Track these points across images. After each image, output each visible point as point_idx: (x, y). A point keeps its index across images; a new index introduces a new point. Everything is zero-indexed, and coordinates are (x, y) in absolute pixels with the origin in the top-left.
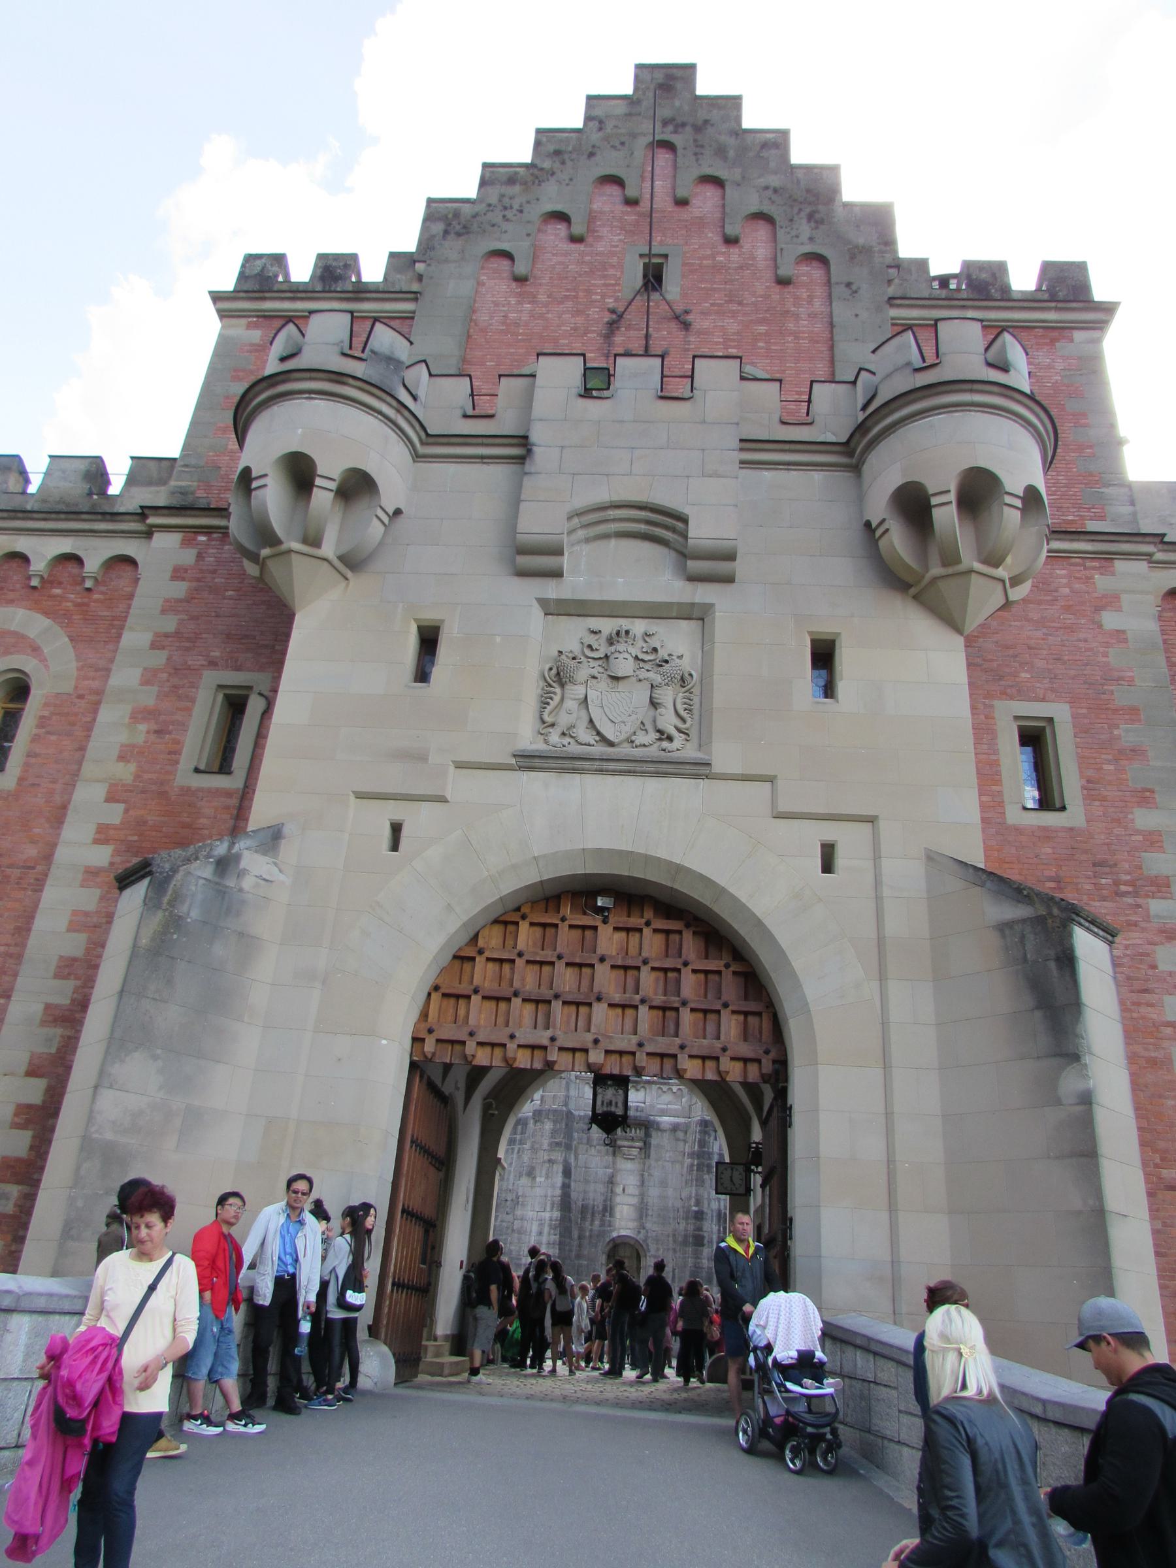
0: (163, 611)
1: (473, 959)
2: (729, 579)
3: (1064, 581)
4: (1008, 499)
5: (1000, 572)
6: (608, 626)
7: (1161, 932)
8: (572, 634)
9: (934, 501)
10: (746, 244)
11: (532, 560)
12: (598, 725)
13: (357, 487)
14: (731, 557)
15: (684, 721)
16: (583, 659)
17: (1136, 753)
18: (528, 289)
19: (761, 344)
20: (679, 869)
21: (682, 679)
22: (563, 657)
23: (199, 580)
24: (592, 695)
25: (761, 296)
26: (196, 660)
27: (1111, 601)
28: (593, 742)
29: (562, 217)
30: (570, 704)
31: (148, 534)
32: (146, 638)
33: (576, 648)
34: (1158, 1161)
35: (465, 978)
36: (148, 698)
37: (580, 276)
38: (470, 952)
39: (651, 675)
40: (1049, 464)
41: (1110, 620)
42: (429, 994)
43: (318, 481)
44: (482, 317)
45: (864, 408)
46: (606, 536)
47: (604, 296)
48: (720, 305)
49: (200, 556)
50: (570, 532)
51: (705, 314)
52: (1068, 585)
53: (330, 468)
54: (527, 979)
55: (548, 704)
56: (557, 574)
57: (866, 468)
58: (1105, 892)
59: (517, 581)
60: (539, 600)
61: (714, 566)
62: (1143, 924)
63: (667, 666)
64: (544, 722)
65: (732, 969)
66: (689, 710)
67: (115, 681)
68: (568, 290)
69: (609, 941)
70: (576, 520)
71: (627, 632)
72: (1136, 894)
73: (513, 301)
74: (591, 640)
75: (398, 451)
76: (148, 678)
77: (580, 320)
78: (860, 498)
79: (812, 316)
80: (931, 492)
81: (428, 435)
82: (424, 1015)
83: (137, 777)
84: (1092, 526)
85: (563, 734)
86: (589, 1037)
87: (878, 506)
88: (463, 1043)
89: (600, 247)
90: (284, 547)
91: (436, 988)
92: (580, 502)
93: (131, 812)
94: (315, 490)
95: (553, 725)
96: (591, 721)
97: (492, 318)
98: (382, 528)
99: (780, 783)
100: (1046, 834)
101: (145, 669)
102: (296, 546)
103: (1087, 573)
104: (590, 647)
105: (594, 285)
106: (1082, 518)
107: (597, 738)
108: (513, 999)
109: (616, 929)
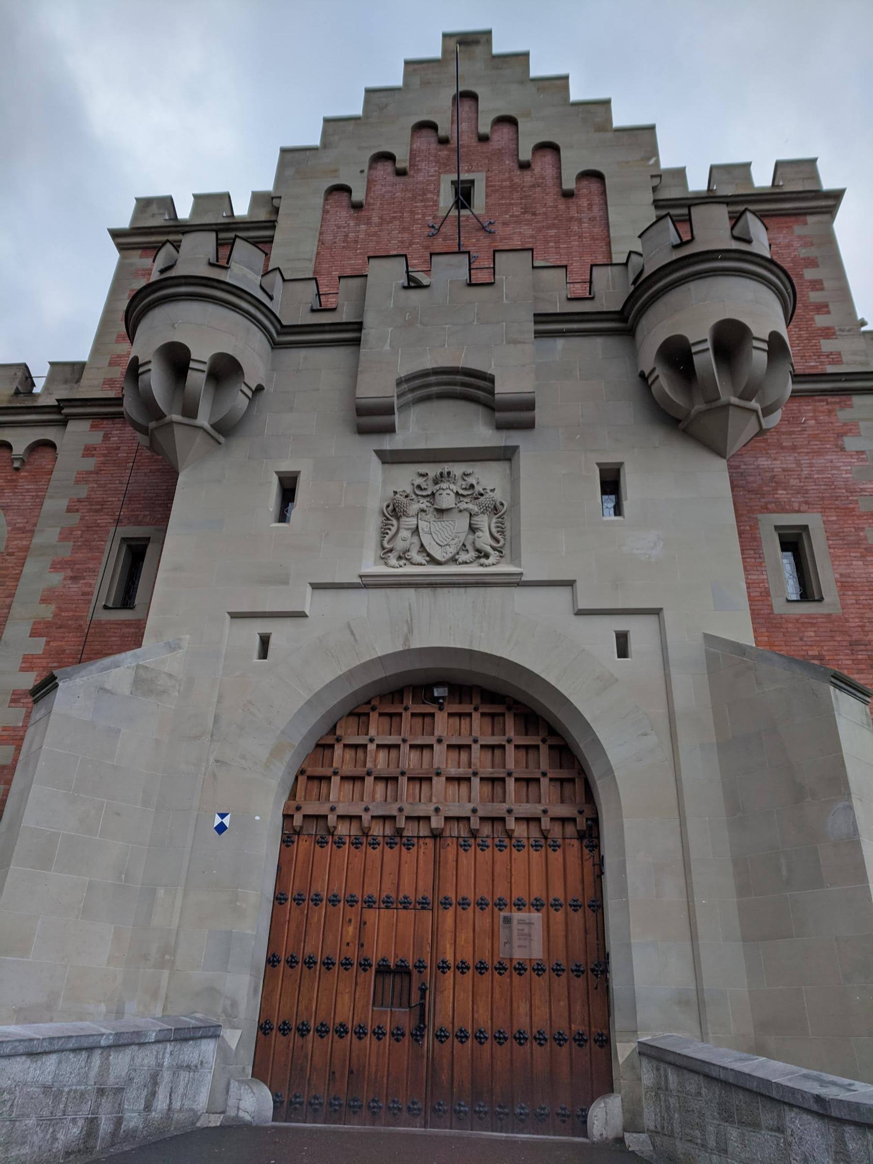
0: (77, 482)
1: (332, 746)
2: (529, 425)
3: (811, 415)
4: (756, 343)
5: (754, 404)
6: (433, 470)
8: (405, 478)
9: (694, 349)
10: (537, 168)
11: (371, 420)
12: (427, 548)
13: (225, 370)
14: (529, 406)
15: (498, 541)
16: (414, 496)
18: (363, 213)
19: (551, 244)
21: (495, 508)
22: (398, 496)
23: (105, 455)
24: (423, 525)
25: (550, 207)
26: (104, 519)
28: (424, 562)
30: (404, 534)
31: (63, 423)
32: (64, 503)
33: (409, 490)
35: (327, 762)
36: (66, 552)
37: (405, 200)
38: (330, 740)
39: (470, 506)
40: (789, 320)
41: (851, 443)
42: (297, 778)
43: (192, 365)
45: (634, 283)
46: (428, 398)
47: (424, 215)
48: (517, 216)
49: (106, 437)
51: (505, 224)
52: (815, 418)
53: (202, 352)
54: (380, 762)
55: (387, 534)
56: (390, 429)
57: (639, 335)
59: (357, 437)
60: (375, 451)
61: (517, 415)
63: (482, 498)
64: (383, 548)
65: (549, 742)
66: (502, 533)
67: (37, 540)
68: (395, 212)
69: (442, 724)
70: (405, 386)
71: (449, 473)
73: (352, 223)
74: (420, 481)
75: (258, 339)
76: (66, 535)
78: (634, 354)
79: (592, 219)
80: (691, 341)
81: (283, 326)
82: (293, 795)
83: (56, 615)
84: (830, 369)
85: (400, 558)
86: (432, 807)
87: (648, 359)
88: (325, 817)
89: (420, 177)
90: (168, 418)
91: (302, 772)
93: (51, 643)
94: (190, 371)
95: (391, 551)
96: (422, 545)
97: (335, 237)
98: (247, 401)
99: (578, 585)
100: (810, 622)
101: (62, 528)
102: (176, 417)
103: (829, 407)
104: (419, 487)
105: (416, 207)
106: (822, 363)
107: (428, 559)
108: (367, 779)
109: (450, 715)
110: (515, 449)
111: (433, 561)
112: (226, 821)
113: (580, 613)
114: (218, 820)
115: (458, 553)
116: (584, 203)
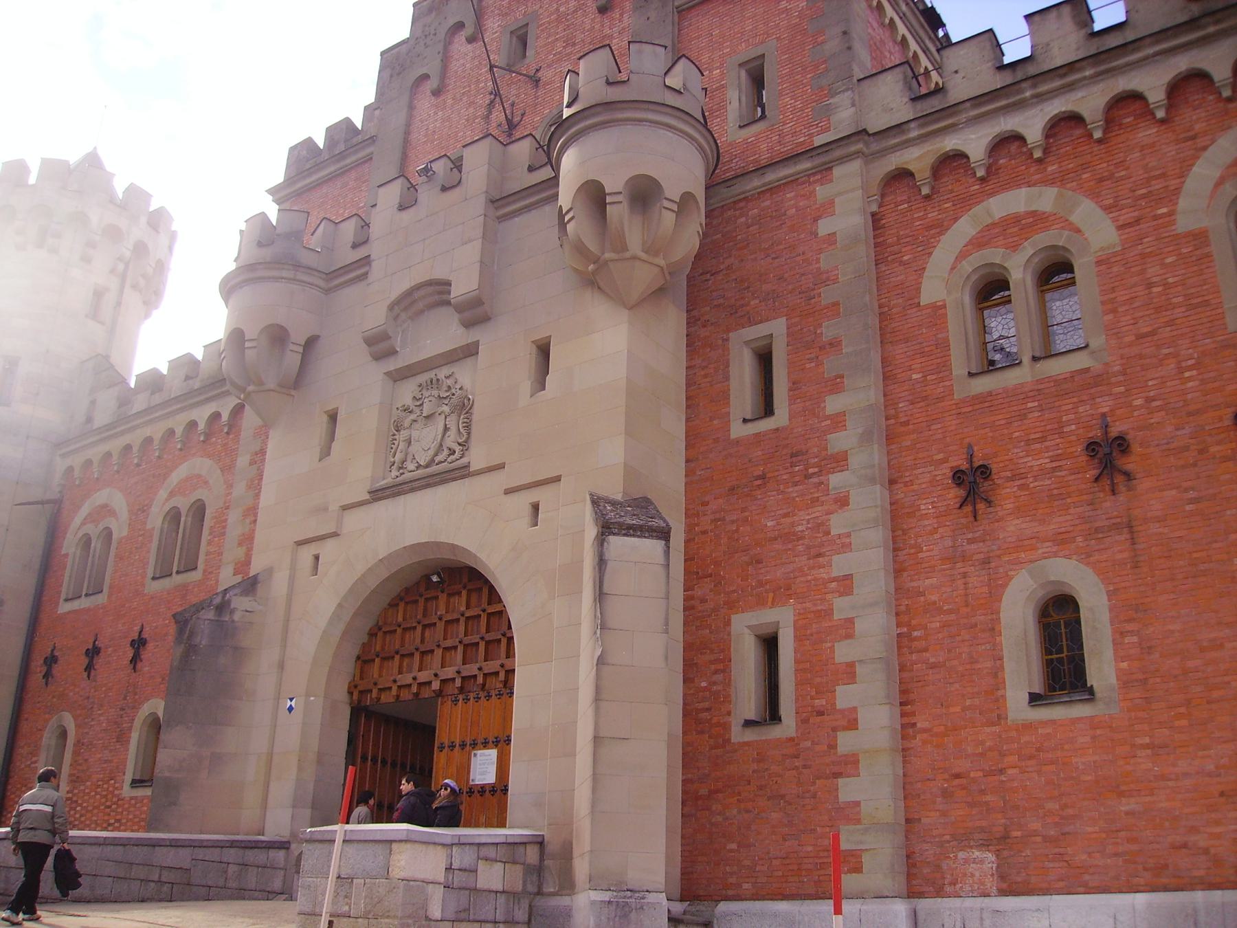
2: (485, 319)
6: (423, 378)
7: (836, 501)
8: (407, 392)
11: (380, 346)
17: (835, 344)
20: (453, 547)
24: (415, 434)
27: (827, 208)
29: (460, 26)
34: (813, 693)
41: (825, 227)
44: (414, 136)
46: (422, 312)
50: (396, 318)
56: (392, 352)
58: (797, 479)
62: (823, 499)
72: (819, 474)
77: (471, 110)
84: (819, 141)
91: (358, 658)
92: (394, 295)
100: (758, 438)
103: (811, 188)
109: (450, 595)
110: (477, 344)
111: (419, 467)
112: (293, 703)
113: (508, 492)
114: (289, 703)
115: (436, 455)
116: (616, 14)
